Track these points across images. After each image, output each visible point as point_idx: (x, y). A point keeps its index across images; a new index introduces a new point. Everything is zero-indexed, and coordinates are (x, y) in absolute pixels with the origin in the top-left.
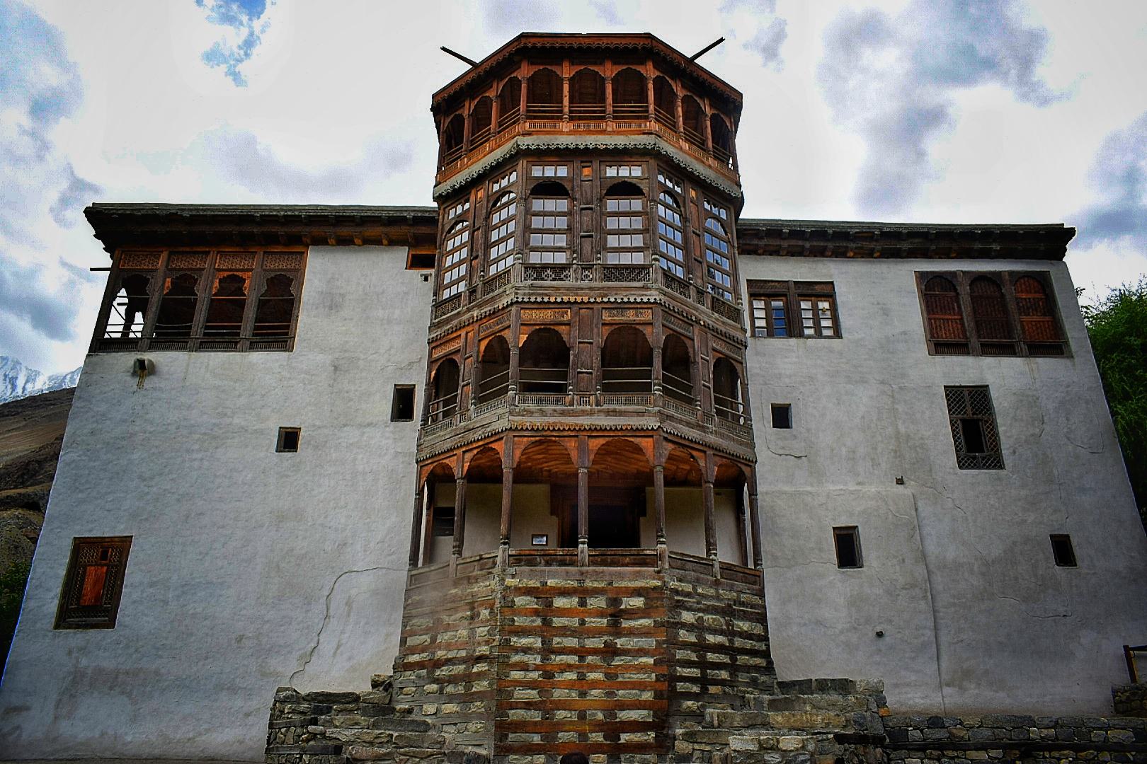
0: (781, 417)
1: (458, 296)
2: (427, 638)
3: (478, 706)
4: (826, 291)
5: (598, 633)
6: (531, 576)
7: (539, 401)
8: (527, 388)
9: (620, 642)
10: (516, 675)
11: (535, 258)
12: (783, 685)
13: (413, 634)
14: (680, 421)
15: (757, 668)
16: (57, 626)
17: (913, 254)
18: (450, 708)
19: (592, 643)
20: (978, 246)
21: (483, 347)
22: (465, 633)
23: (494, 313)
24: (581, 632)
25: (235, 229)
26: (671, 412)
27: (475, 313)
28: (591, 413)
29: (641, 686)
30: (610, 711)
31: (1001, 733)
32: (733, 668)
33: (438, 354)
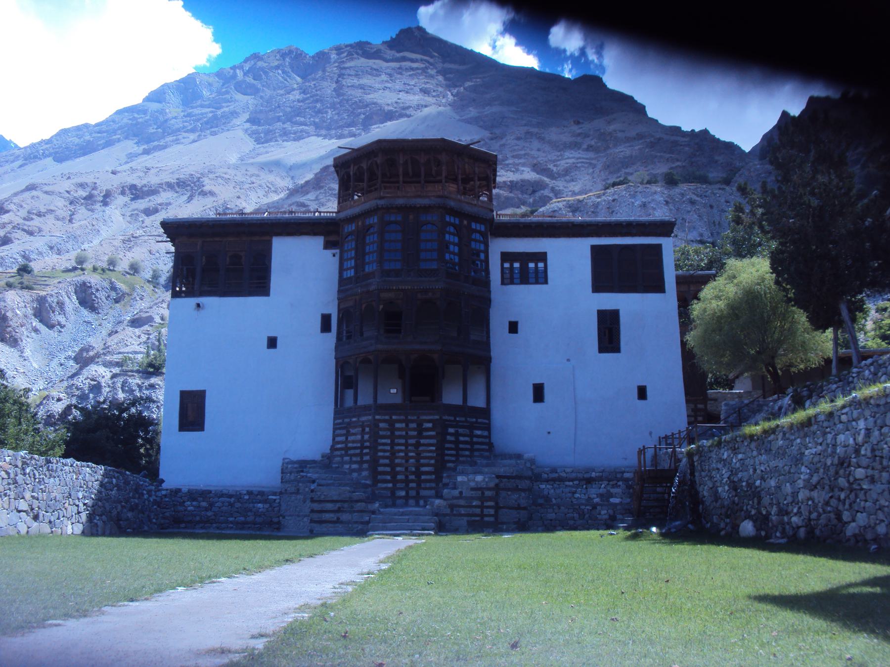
0: (513, 327)
1: (350, 278)
3: (365, 466)
4: (542, 257)
5: (412, 437)
9: (422, 441)
10: (380, 454)
15: (483, 450)
18: (355, 466)
19: (411, 441)
24: (407, 437)
30: (417, 468)
32: (472, 450)
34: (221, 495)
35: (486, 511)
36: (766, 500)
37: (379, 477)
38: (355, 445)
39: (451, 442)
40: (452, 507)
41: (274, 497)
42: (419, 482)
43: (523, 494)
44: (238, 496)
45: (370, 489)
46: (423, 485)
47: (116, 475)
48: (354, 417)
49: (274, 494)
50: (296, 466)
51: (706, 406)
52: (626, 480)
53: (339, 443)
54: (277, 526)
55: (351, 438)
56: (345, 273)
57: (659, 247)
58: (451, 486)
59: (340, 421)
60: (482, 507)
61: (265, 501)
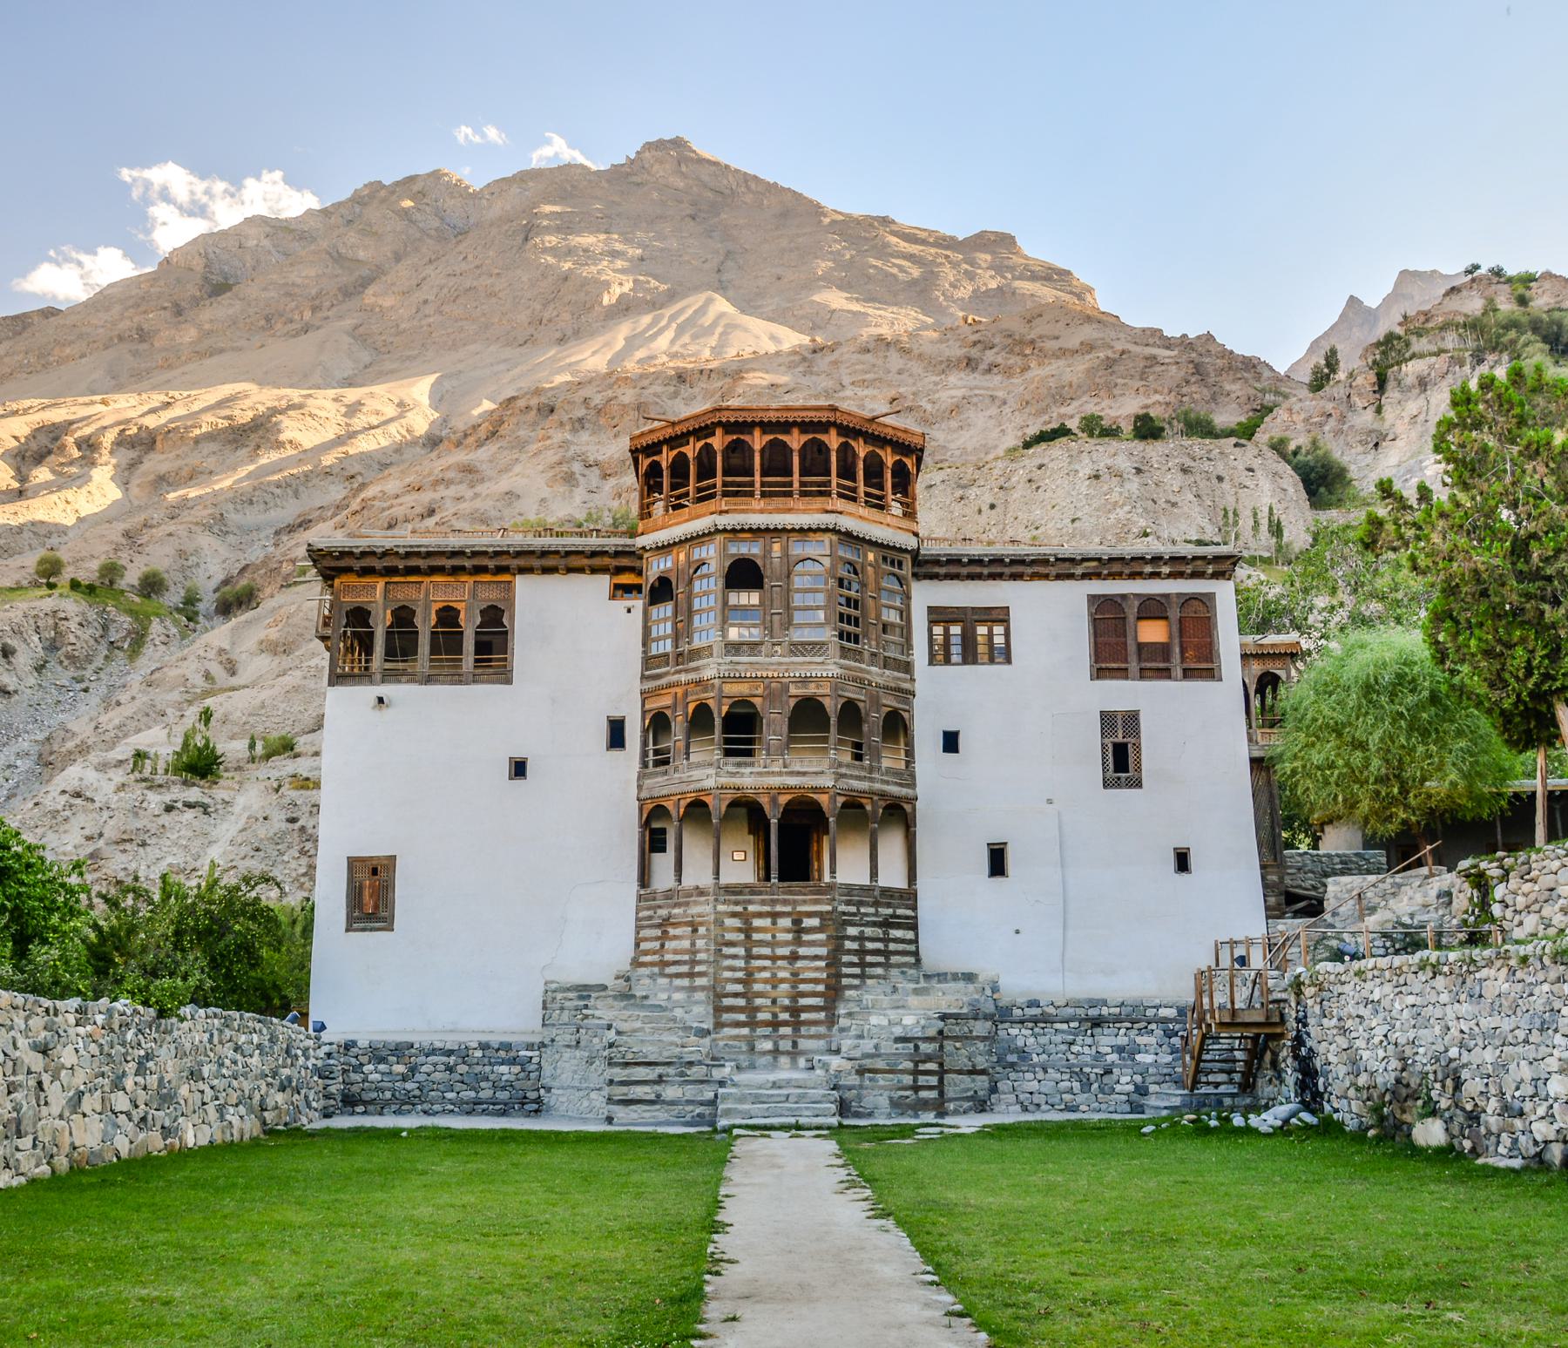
0: (951, 742)
1: (666, 655)
2: (657, 945)
3: (700, 996)
4: (999, 616)
5: (786, 944)
6: (737, 903)
7: (739, 765)
8: (728, 753)
9: (802, 951)
10: (727, 974)
11: (733, 634)
12: (927, 977)
13: (646, 939)
14: (852, 777)
16: (347, 930)
17: (1086, 576)
18: (678, 996)
19: (781, 951)
20: (1148, 569)
21: (690, 710)
22: (686, 944)
23: (699, 682)
24: (773, 944)
25: (448, 563)
26: (843, 770)
27: (683, 678)
28: (780, 774)
29: (816, 981)
31: (1081, 1012)
32: (887, 965)
33: (653, 704)
34: (434, 1051)
35: (922, 1080)
36: (1473, 1086)
37: (726, 1017)
38: (678, 958)
39: (849, 952)
40: (861, 1072)
41: (529, 1054)
42: (797, 1025)
43: (981, 1046)
44: (463, 1054)
45: (707, 1041)
46: (803, 1030)
47: (258, 1026)
48: (676, 905)
49: (530, 1047)
50: (571, 995)
51: (1281, 879)
52: (1165, 1020)
53: (646, 953)
54: (535, 1106)
55: (670, 945)
56: (654, 645)
57: (1207, 601)
58: (853, 1033)
59: (650, 913)
60: (916, 1073)
61: (513, 1062)
